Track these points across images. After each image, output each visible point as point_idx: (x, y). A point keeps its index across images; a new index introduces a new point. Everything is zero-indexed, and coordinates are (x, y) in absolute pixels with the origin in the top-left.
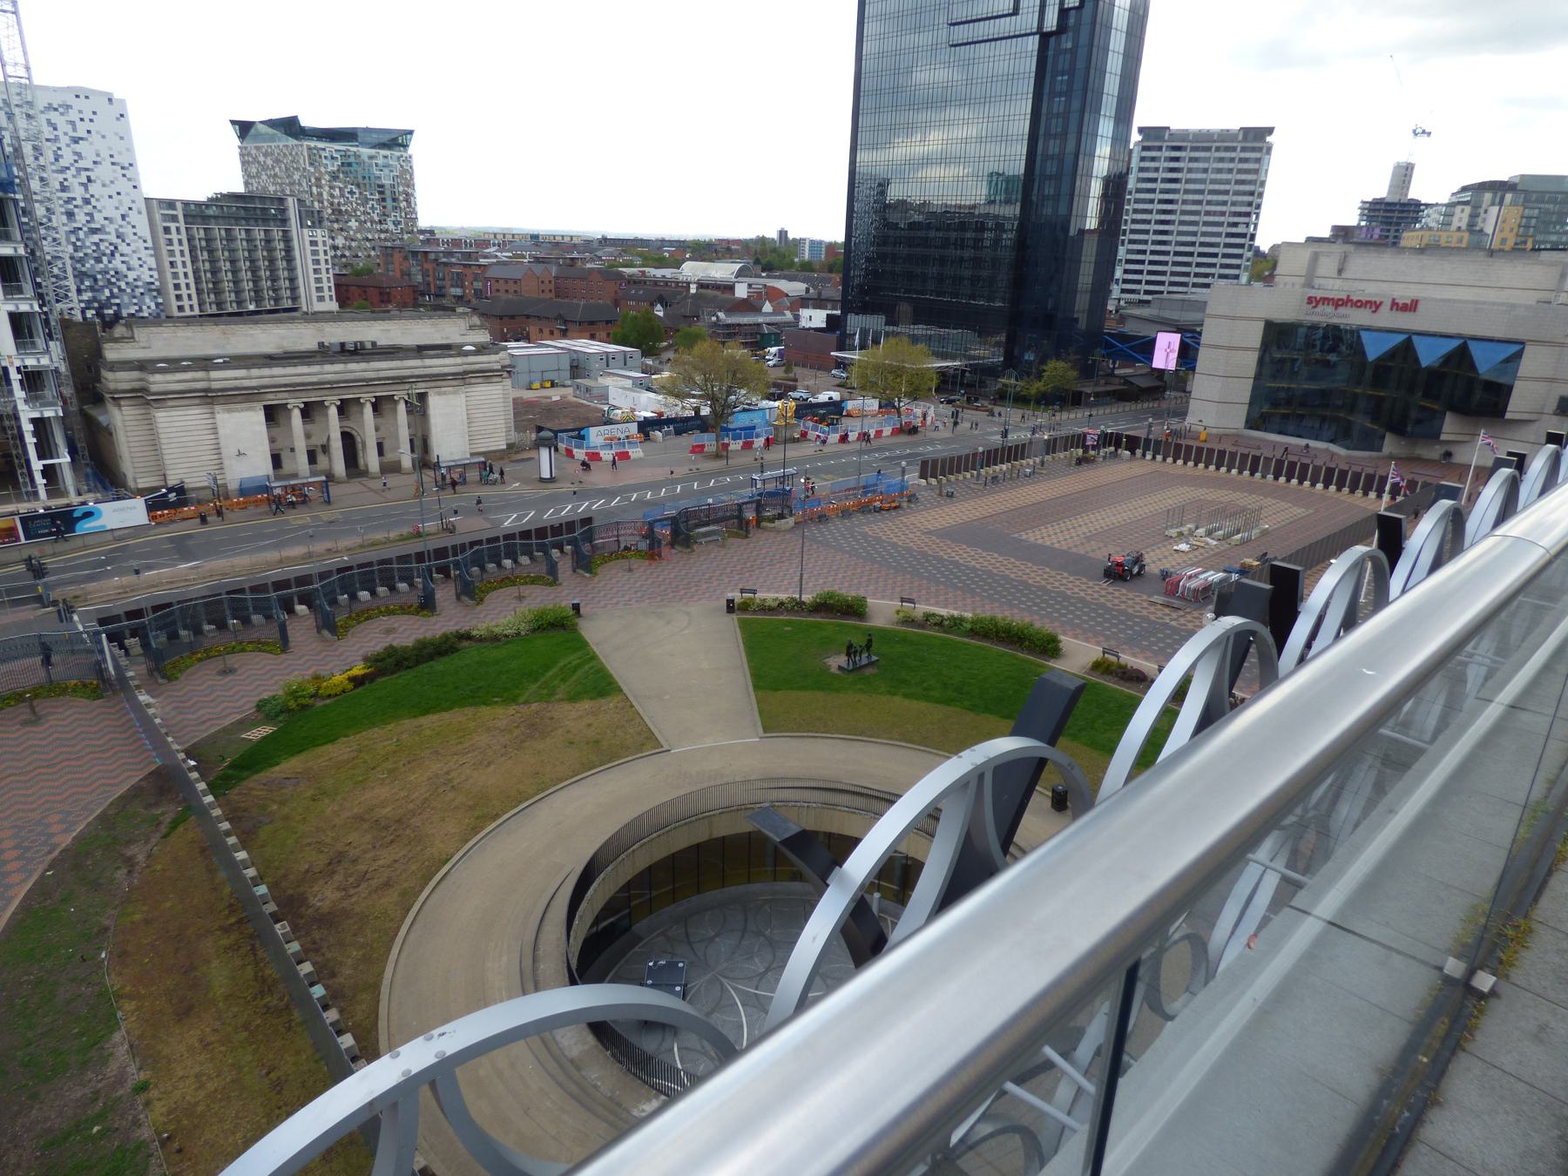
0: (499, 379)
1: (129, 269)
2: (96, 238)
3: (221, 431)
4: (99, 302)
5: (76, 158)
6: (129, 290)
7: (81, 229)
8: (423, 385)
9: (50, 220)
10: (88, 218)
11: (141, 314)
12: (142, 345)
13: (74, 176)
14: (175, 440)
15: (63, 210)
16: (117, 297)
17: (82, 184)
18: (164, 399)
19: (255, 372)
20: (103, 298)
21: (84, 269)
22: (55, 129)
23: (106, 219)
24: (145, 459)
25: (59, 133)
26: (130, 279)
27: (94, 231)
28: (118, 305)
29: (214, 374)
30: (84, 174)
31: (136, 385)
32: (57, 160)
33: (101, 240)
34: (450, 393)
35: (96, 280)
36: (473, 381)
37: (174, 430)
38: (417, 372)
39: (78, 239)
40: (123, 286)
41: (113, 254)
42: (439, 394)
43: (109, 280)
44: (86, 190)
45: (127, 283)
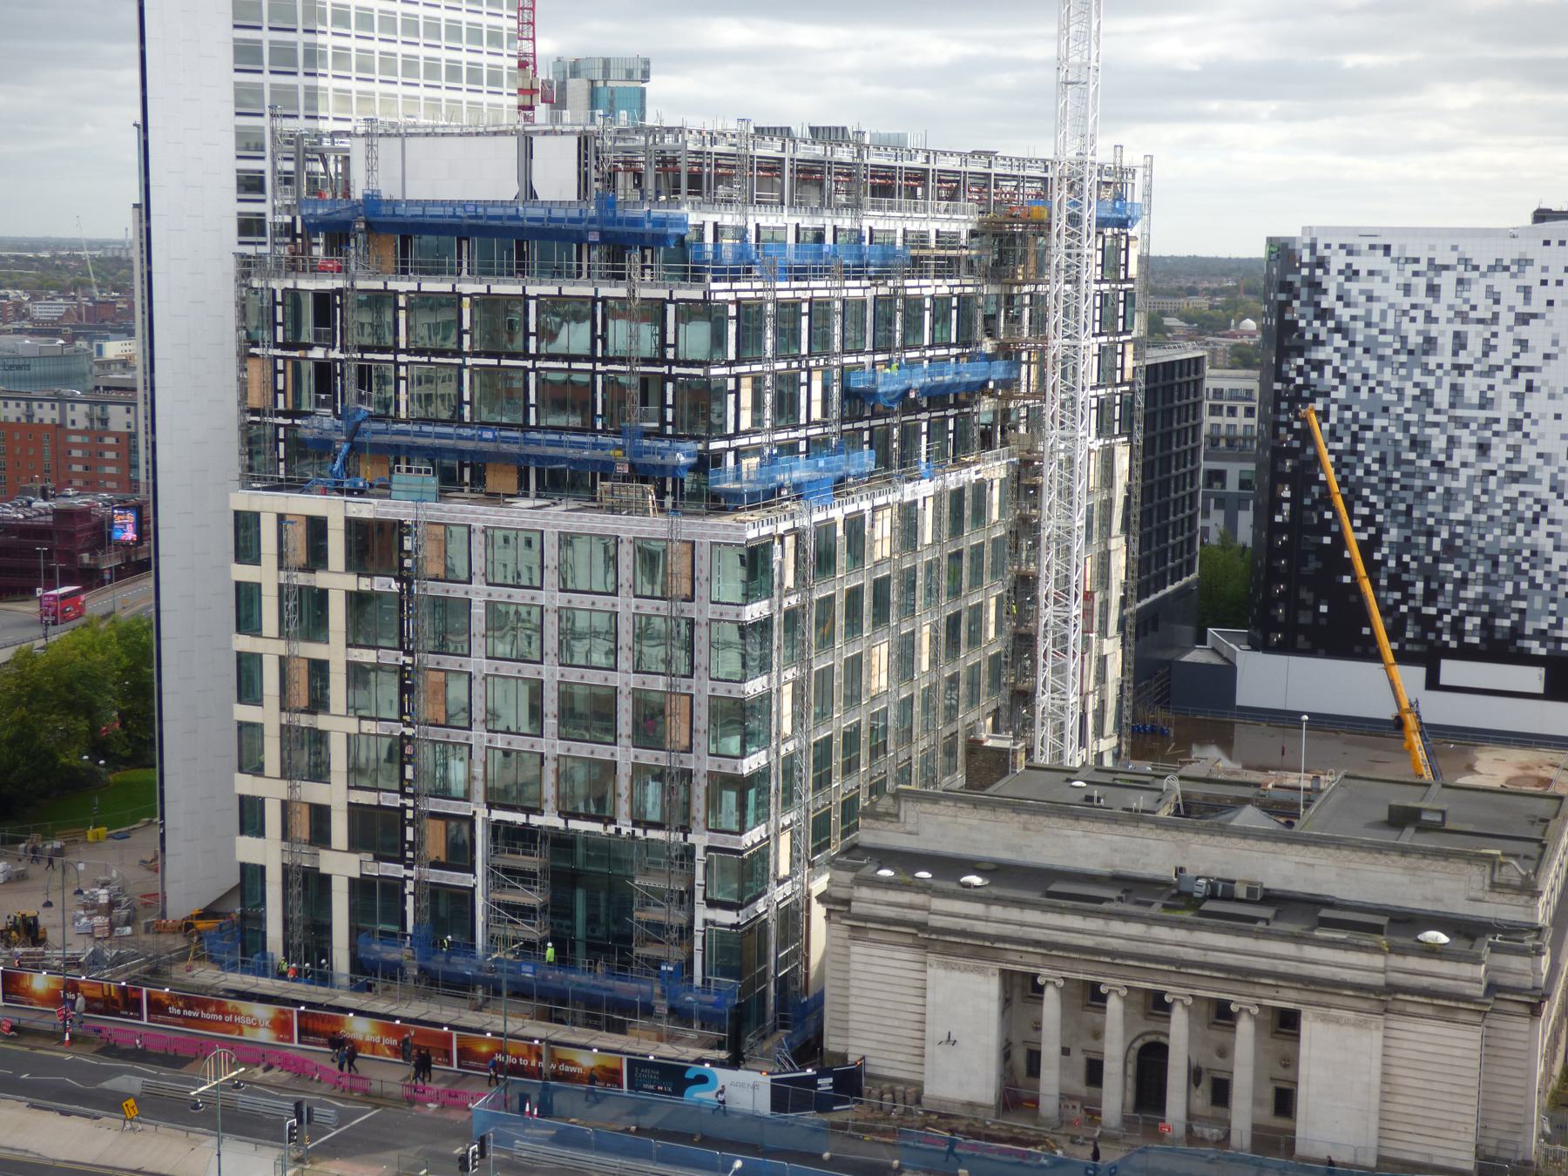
0: (1478, 1019)
1: (1557, 548)
2: (1513, 490)
3: (929, 995)
4: (1493, 603)
5: (1517, 349)
6: (1547, 587)
7: (1493, 473)
8: (1293, 994)
9: (1450, 457)
10: (1511, 454)
11: (1557, 633)
12: (908, 828)
13: (1506, 382)
14: (868, 993)
15: (1474, 440)
16: (1524, 598)
17: (1516, 395)
19: (997, 911)
20: (1501, 597)
21: (1481, 544)
22: (1497, 302)
23: (1540, 455)
25: (1501, 309)
26: (1554, 567)
27: (1515, 478)
28: (1522, 612)
30: (1523, 377)
32: (1485, 354)
33: (1523, 494)
34: (1347, 1023)
35: (1496, 564)
36: (1411, 1009)
37: (870, 977)
38: (1282, 967)
39: (1485, 492)
40: (1539, 576)
41: (1536, 520)
42: (1326, 1019)
43: (1518, 566)
44: (1520, 405)
45: (1548, 574)
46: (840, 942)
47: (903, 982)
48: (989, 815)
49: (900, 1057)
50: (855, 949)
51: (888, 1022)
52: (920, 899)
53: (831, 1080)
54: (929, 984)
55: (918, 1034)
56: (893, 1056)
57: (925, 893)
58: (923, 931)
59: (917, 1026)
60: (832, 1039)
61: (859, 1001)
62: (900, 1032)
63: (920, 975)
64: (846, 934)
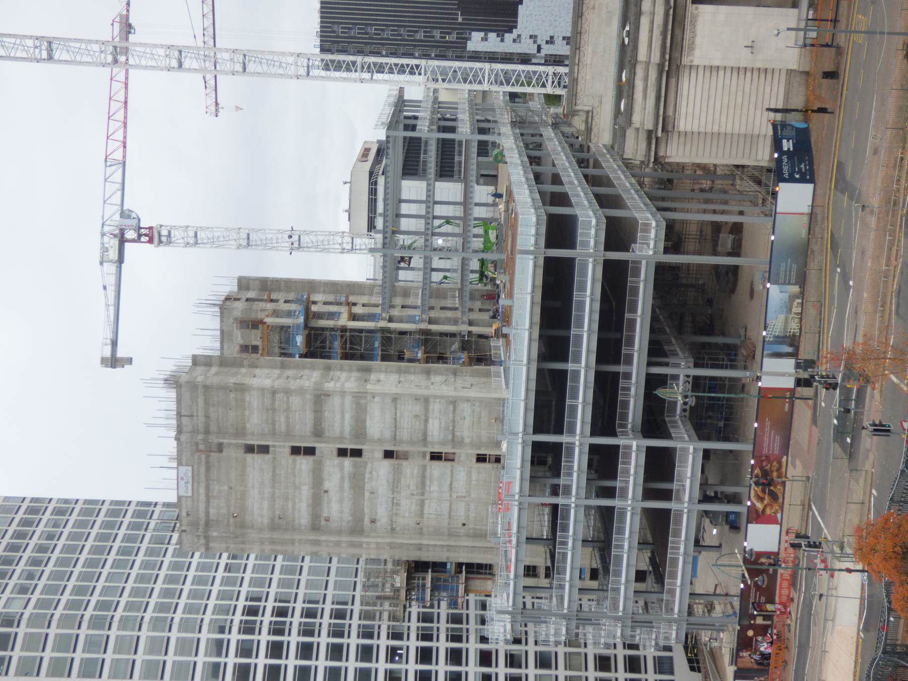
3: (716, 63)
12: (597, 104)
14: (717, 117)
24: (734, 145)
29: (642, 55)
31: (643, 136)
37: (703, 115)
46: (681, 148)
47: (706, 86)
48: (584, 37)
49: (768, 90)
51: (739, 100)
53: (784, 141)
54: (707, 63)
55: (749, 74)
59: (742, 76)
60: (760, 157)
61: (723, 124)
62: (747, 90)
63: (701, 71)
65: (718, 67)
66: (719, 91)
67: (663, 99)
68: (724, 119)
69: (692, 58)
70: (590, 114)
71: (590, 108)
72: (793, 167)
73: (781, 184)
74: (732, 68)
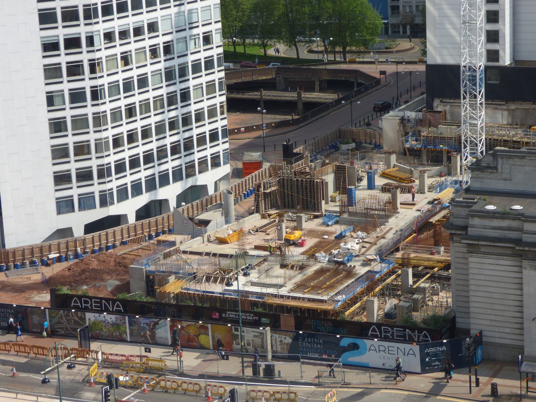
12: (504, 176)
18: (478, 245)
37: (483, 277)
46: (461, 255)
47: (506, 280)
49: (507, 330)
50: (471, 259)
52: (515, 224)
54: (525, 281)
55: (519, 315)
56: (502, 330)
57: (519, 219)
58: (517, 245)
59: (517, 309)
61: (476, 294)
64: (465, 250)
65: (522, 290)
66: (503, 291)
67: (493, 244)
68: (481, 294)
69: (528, 268)
70: (495, 171)
71: (500, 170)
72: (435, 355)
73: (418, 346)
74: (522, 301)
